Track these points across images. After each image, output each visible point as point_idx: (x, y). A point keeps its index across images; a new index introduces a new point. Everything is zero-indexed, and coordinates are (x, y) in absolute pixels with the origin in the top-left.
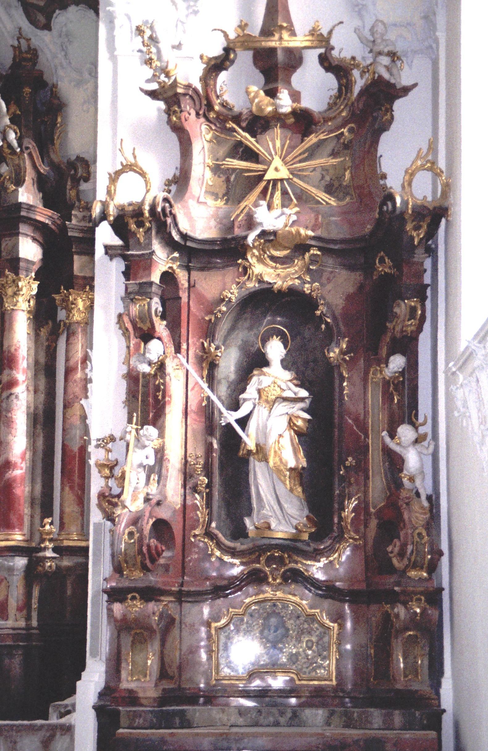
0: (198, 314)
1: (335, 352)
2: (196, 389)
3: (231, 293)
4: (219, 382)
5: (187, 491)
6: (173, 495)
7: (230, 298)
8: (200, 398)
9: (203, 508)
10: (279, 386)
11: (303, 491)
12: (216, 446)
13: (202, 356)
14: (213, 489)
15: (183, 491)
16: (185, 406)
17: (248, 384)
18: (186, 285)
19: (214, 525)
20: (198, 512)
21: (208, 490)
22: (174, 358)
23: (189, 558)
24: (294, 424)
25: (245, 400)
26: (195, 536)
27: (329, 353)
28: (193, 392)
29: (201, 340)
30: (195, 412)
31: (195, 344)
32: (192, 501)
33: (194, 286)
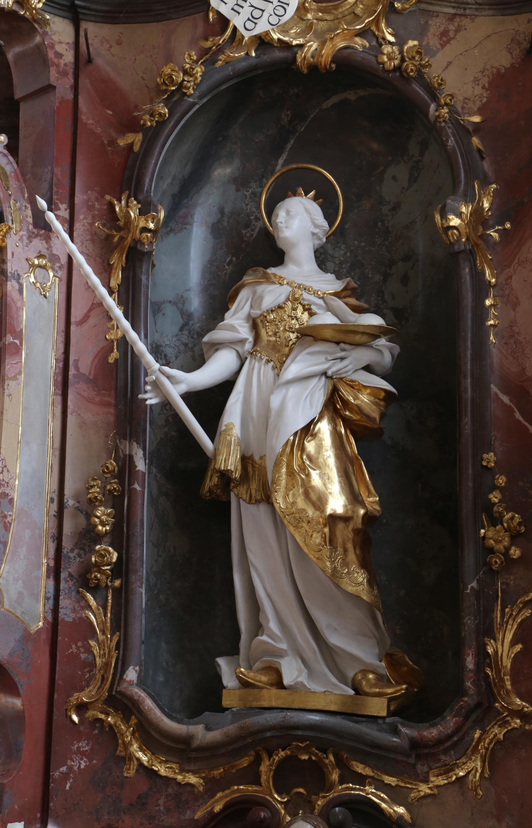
0: (99, 130)
1: (459, 215)
2: (92, 321)
3: (186, 72)
4: (157, 308)
5: (63, 585)
6: (20, 594)
7: (181, 85)
8: (103, 343)
9: (103, 632)
10: (307, 309)
11: (369, 582)
12: (141, 465)
13: (108, 238)
14: (133, 578)
15: (51, 583)
16: (61, 365)
17: (228, 309)
18: (69, 57)
19: (131, 674)
20: (92, 643)
21: (117, 583)
22: (31, 237)
23: (64, 769)
24: (346, 403)
25: (216, 346)
26: (81, 708)
27: (444, 216)
28: (86, 326)
29: (108, 197)
30: (88, 381)
31: (91, 208)
32: (74, 610)
33: (90, 60)
